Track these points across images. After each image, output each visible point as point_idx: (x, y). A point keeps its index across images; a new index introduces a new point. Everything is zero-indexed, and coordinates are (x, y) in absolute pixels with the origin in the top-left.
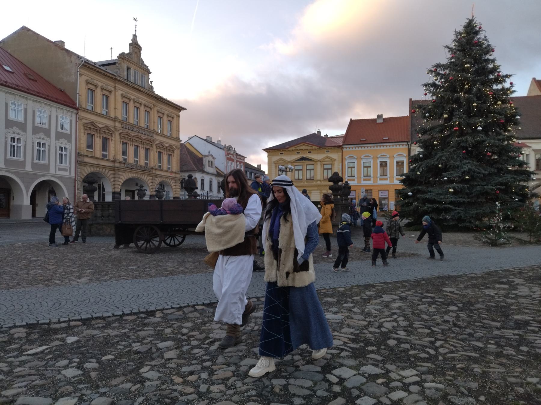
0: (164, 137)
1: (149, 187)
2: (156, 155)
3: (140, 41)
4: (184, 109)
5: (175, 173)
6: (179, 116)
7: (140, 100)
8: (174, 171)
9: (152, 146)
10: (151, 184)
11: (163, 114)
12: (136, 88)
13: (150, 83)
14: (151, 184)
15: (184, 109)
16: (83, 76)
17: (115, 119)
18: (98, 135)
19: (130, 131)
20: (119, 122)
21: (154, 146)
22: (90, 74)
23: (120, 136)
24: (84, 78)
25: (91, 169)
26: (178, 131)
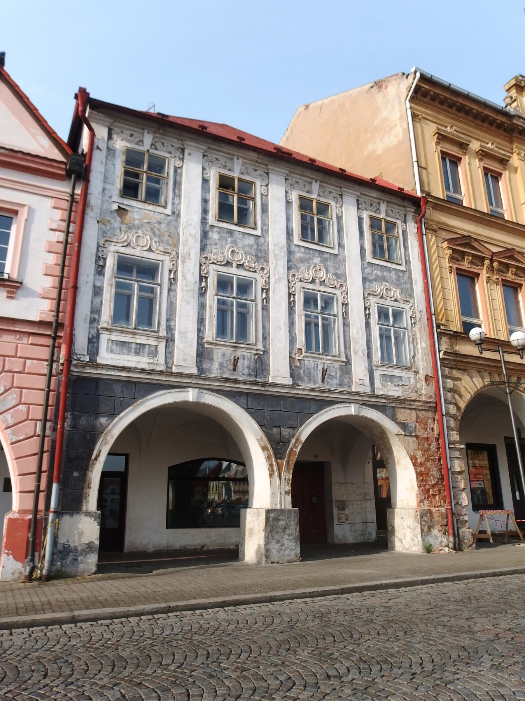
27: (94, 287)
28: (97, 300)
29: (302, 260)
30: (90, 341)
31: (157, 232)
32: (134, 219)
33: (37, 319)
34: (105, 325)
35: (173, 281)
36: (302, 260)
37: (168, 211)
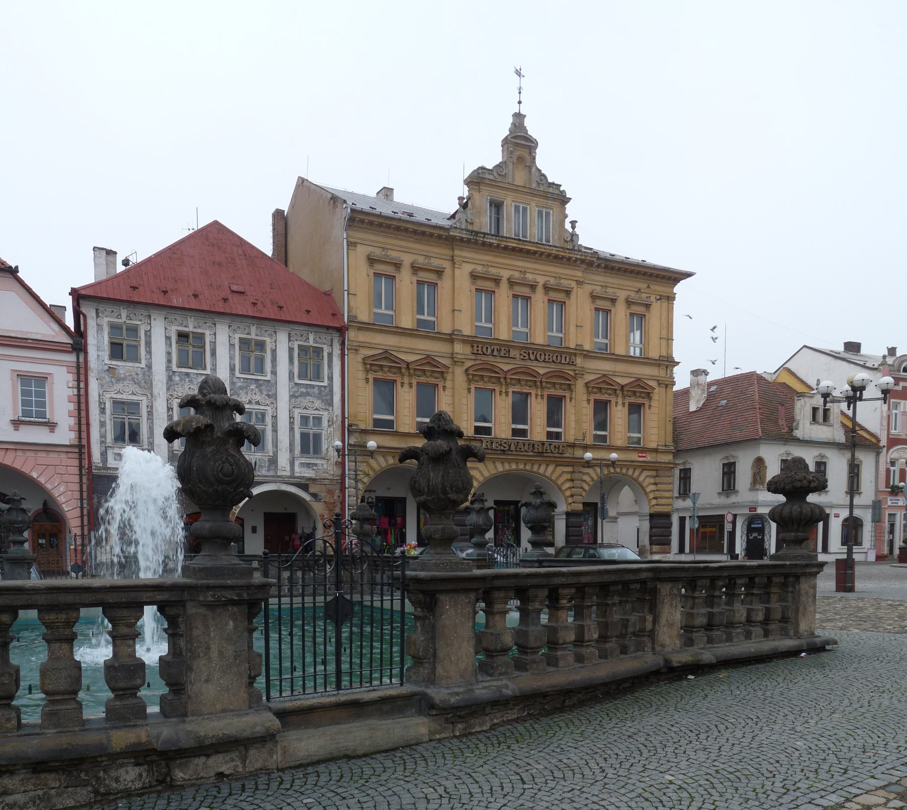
0: (616, 360)
1: (563, 492)
2: (588, 411)
3: (533, 128)
4: (688, 275)
5: (656, 451)
6: (670, 298)
7: (529, 276)
8: (653, 445)
9: (569, 387)
10: (568, 485)
11: (613, 301)
12: (514, 249)
13: (568, 226)
14: (568, 485)
15: (688, 275)
16: (359, 247)
17: (450, 338)
18: (406, 380)
19: (499, 360)
20: (464, 342)
21: (580, 387)
22: (379, 239)
23: (468, 375)
24: (362, 251)
25: (386, 461)
26: (669, 339)
27: (100, 421)
28: (103, 430)
29: (241, 388)
30: (102, 454)
31: (136, 381)
32: (120, 374)
33: (68, 443)
34: (110, 445)
35: (150, 413)
36: (241, 388)
37: (143, 365)
